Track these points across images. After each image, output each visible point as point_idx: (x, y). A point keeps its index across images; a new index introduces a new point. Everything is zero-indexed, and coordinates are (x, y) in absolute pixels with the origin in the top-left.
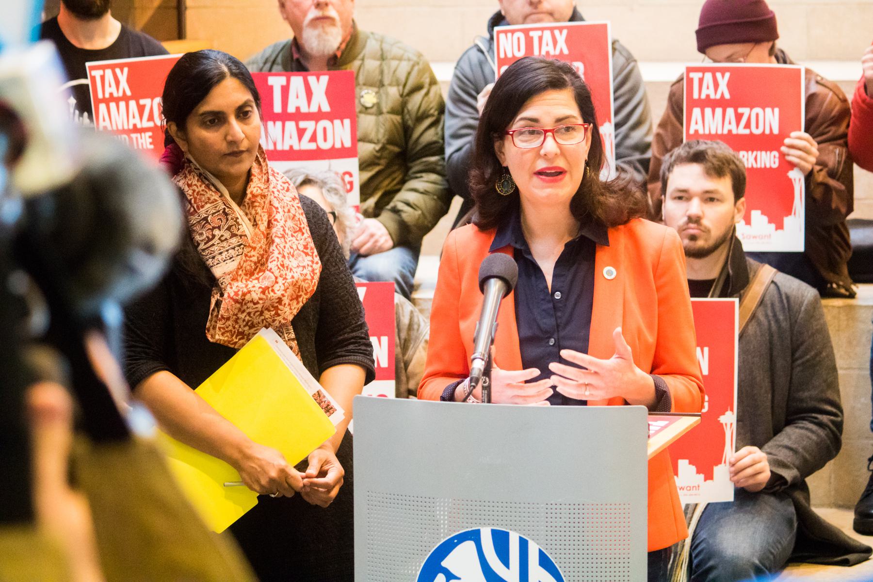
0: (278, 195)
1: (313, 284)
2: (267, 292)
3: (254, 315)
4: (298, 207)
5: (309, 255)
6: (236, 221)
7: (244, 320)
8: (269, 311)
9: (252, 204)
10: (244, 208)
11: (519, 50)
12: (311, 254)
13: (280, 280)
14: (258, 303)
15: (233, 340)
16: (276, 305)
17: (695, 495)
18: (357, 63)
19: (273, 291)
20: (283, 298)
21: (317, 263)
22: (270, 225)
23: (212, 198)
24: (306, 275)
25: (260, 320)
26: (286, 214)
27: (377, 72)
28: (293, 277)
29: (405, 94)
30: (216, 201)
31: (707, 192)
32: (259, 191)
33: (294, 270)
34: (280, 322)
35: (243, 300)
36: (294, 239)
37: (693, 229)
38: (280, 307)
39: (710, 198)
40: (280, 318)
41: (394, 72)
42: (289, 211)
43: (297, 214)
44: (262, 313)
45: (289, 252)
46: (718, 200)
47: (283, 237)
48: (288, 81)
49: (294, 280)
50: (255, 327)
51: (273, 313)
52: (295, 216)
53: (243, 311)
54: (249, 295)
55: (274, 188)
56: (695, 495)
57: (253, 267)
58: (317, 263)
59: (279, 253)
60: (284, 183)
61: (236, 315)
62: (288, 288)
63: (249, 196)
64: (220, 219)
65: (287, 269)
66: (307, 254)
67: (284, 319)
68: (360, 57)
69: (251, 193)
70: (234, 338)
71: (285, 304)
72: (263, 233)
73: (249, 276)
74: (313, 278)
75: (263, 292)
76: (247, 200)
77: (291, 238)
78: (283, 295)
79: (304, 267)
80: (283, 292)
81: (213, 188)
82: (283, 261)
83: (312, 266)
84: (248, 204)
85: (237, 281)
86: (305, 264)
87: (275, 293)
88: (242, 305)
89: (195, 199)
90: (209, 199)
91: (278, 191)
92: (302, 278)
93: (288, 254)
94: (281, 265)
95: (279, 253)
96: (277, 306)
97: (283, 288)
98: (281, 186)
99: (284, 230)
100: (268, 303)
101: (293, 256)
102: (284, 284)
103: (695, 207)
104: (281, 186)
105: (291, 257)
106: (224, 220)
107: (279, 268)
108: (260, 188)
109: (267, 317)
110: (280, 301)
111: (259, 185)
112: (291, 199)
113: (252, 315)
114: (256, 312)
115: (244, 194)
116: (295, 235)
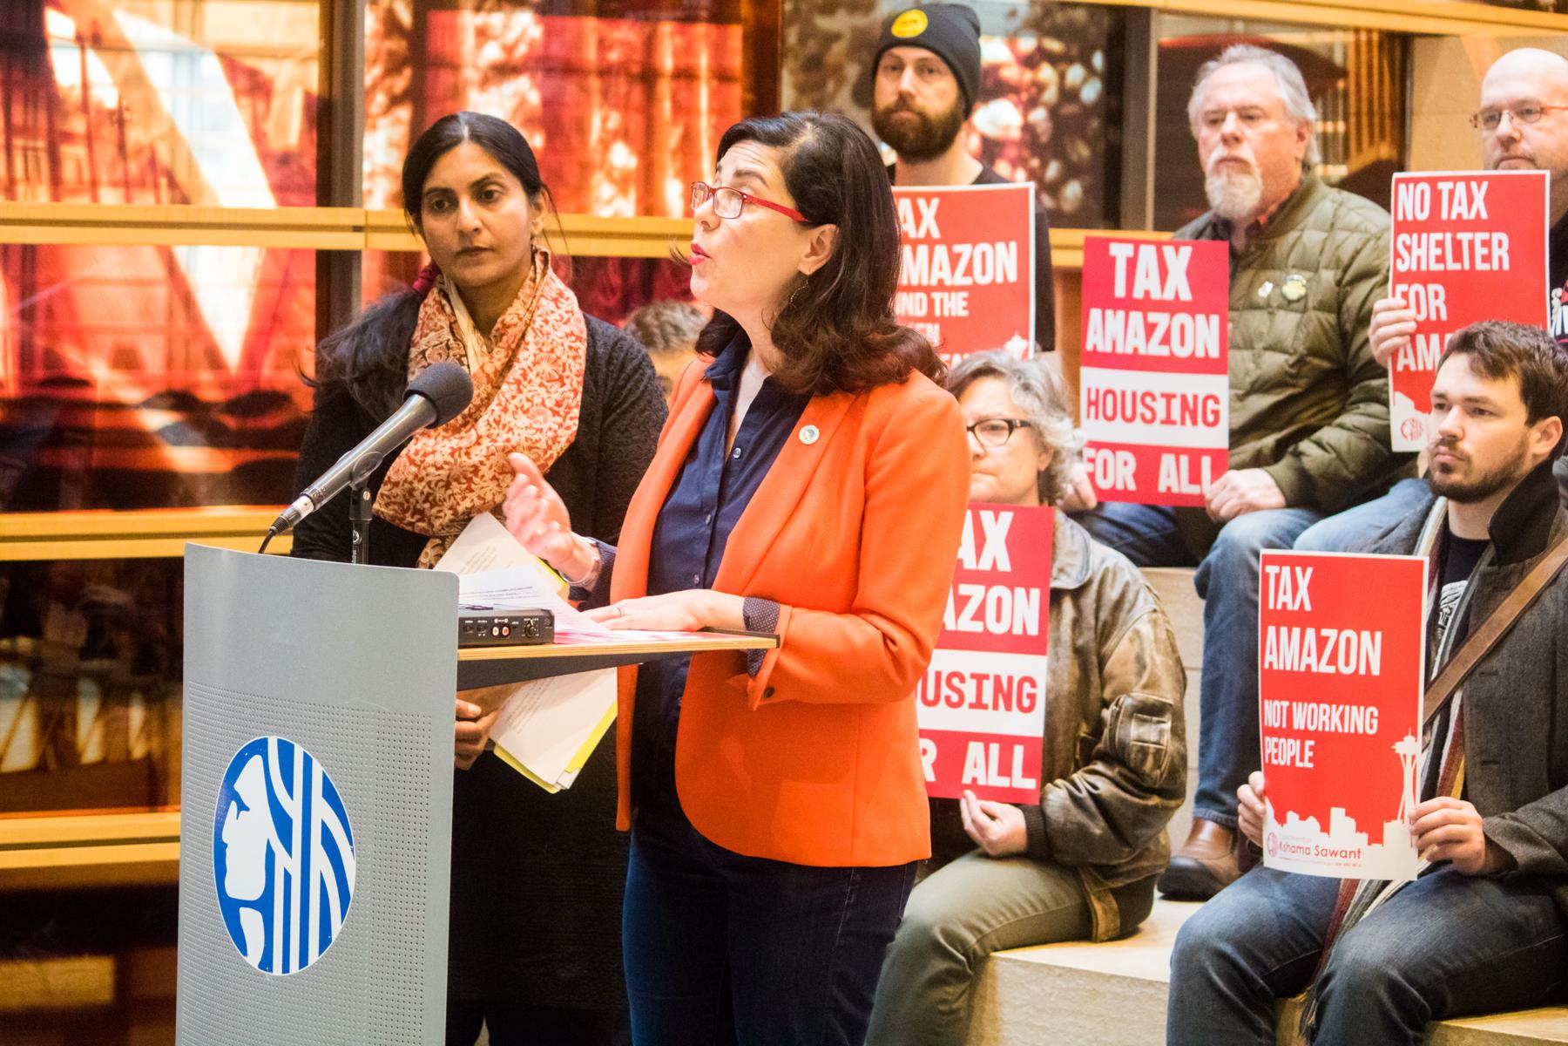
0: (542, 326)
1: (547, 456)
2: (457, 454)
3: (436, 485)
4: (570, 348)
5: (559, 415)
6: (459, 360)
7: (422, 493)
8: (460, 483)
9: (499, 338)
10: (488, 343)
11: (1422, 210)
12: (562, 414)
13: (486, 442)
14: (441, 468)
15: (404, 519)
16: (470, 475)
17: (1354, 865)
18: (1292, 236)
19: (468, 454)
20: (481, 467)
21: (568, 428)
22: (508, 366)
23: (439, 324)
24: (537, 441)
25: (446, 496)
26: (542, 354)
27: (1317, 250)
28: (508, 440)
29: (1345, 281)
30: (442, 328)
31: (1476, 400)
32: (516, 320)
33: (516, 431)
34: (472, 500)
35: (422, 462)
36: (542, 391)
37: (1444, 454)
38: (476, 480)
39: (1477, 408)
40: (473, 496)
41: (1338, 247)
42: (552, 351)
43: (564, 358)
44: (448, 486)
45: (519, 405)
46: (1491, 414)
47: (518, 382)
48: (1136, 252)
49: (508, 445)
50: (437, 505)
51: (464, 486)
52: (559, 358)
53: (421, 480)
54: (432, 456)
55: (540, 316)
56: (1354, 865)
57: (460, 422)
58: (568, 428)
59: (499, 404)
60: (567, 312)
61: (411, 483)
62: (493, 454)
63: (498, 325)
64: (440, 354)
65: (504, 426)
66: (556, 413)
67: (479, 497)
68: (1299, 227)
69: (502, 322)
70: (408, 515)
71: (483, 476)
72: (488, 376)
73: (450, 433)
74: (550, 448)
75: (452, 455)
76: (493, 332)
77: (537, 388)
78: (482, 463)
79: (541, 430)
80: (484, 459)
81: (448, 309)
82: (500, 416)
83: (555, 431)
84: (495, 337)
85: (429, 437)
86: (545, 426)
87: (469, 458)
88: (419, 470)
89: (423, 323)
90: (436, 325)
91: (546, 322)
92: (526, 445)
93: (517, 407)
94: (495, 421)
95: (499, 404)
96: (471, 478)
97: (484, 452)
98: (560, 315)
99: (525, 375)
100: (456, 471)
101: (525, 412)
102: (488, 448)
103: (1451, 421)
104: (560, 315)
105: (519, 411)
106: (444, 356)
107: (489, 424)
108: (518, 315)
109: (456, 491)
110: (476, 470)
111: (519, 312)
112: (563, 335)
113: (433, 485)
114: (439, 481)
115: (495, 322)
116: (548, 385)
